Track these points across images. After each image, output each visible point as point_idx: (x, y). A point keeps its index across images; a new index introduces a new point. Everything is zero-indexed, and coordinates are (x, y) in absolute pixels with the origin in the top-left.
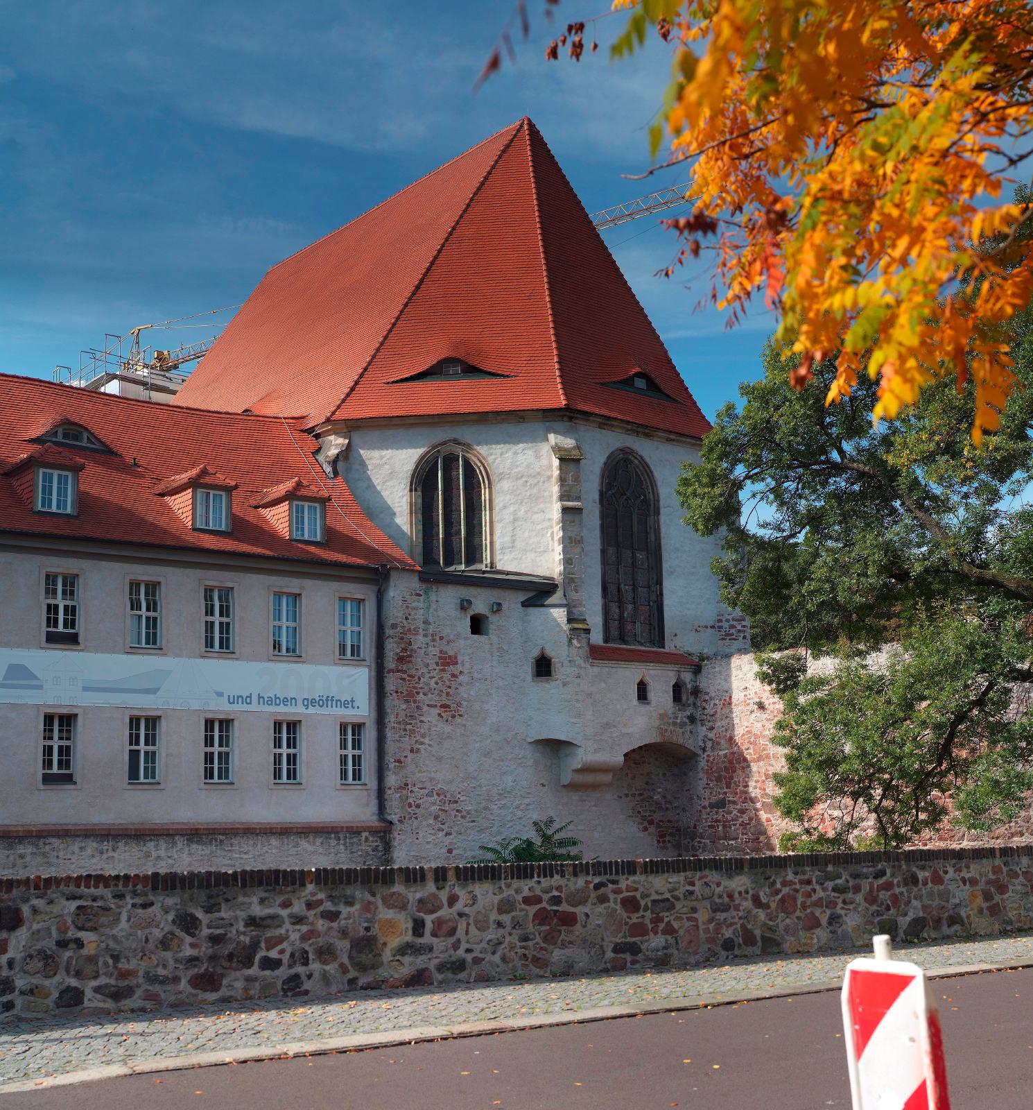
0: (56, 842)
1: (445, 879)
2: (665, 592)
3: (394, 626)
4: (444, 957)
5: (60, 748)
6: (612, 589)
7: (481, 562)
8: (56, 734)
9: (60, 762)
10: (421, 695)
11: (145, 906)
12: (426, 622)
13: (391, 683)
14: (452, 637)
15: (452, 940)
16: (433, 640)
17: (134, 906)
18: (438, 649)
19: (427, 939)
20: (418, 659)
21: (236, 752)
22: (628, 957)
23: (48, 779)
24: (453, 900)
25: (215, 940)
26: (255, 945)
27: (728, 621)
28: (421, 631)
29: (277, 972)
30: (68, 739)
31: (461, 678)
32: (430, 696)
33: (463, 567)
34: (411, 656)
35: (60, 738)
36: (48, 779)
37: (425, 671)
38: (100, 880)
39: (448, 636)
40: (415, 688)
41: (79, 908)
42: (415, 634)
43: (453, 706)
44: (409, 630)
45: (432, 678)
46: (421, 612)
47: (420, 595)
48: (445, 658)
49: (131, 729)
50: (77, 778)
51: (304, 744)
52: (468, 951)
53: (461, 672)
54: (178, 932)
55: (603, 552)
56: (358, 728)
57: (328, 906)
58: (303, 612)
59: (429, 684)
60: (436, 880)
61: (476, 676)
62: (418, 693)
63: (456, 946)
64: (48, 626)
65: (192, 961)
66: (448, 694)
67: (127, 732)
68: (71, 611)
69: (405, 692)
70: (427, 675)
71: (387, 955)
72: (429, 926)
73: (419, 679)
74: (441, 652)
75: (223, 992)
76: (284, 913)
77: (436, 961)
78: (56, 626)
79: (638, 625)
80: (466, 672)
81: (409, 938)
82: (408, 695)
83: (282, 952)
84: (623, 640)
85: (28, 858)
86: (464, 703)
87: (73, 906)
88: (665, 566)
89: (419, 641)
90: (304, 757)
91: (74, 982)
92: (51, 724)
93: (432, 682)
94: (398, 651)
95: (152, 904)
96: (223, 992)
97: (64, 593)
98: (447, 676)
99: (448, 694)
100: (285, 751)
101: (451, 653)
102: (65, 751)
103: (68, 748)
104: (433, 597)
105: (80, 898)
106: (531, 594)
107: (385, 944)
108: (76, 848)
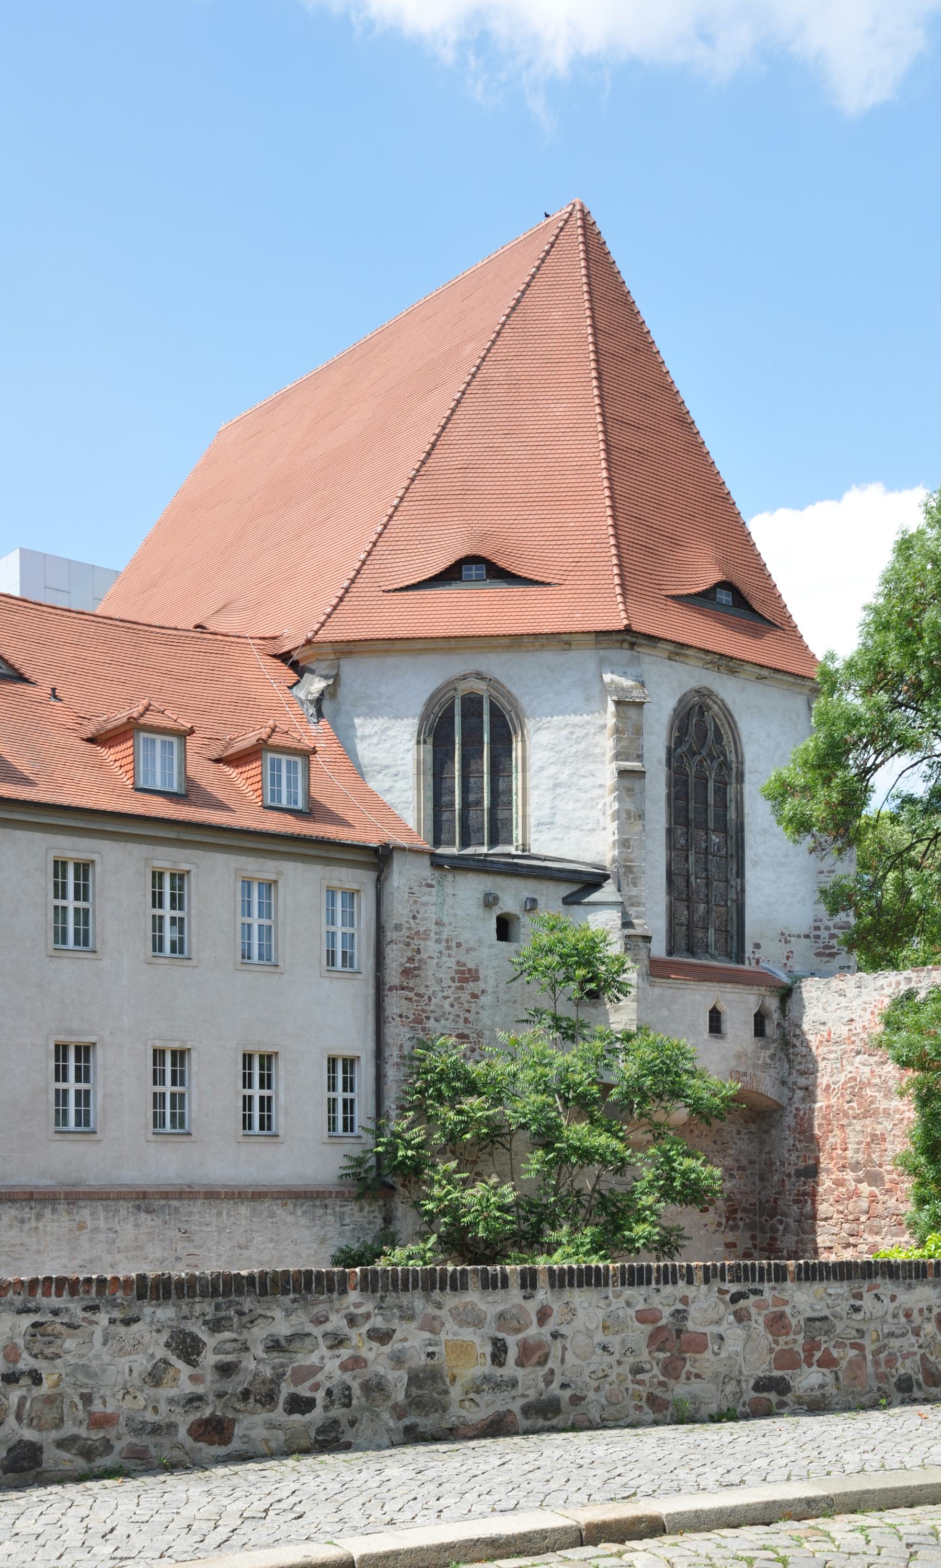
1: (534, 1286)
2: (748, 888)
3: (398, 927)
4: (532, 1394)
6: (680, 882)
7: (510, 842)
10: (432, 1020)
11: (127, 1322)
12: (439, 923)
13: (395, 1004)
14: (472, 944)
15: (543, 1371)
16: (449, 948)
17: (112, 1321)
18: (454, 960)
19: (510, 1369)
20: (430, 972)
21: (195, 1092)
22: (773, 1397)
24: (543, 1315)
25: (226, 1370)
26: (279, 1377)
27: (827, 928)
28: (432, 935)
29: (308, 1417)
31: (484, 1000)
32: (443, 1022)
33: (484, 850)
34: (418, 968)
37: (438, 988)
38: (62, 1285)
39: (466, 942)
40: (424, 1011)
41: (35, 1325)
42: (425, 939)
43: (473, 1036)
44: (418, 933)
45: (446, 998)
46: (433, 908)
47: (431, 886)
48: (462, 972)
49: (57, 1060)
51: (282, 1084)
52: (564, 1386)
53: (483, 992)
54: (173, 1359)
55: (669, 832)
56: (350, 1063)
57: (378, 1322)
58: (280, 905)
59: (442, 1007)
60: (523, 1286)
61: (502, 996)
62: (428, 1018)
63: (548, 1382)
65: (194, 1400)
67: (52, 1064)
69: (412, 1017)
70: (440, 995)
71: (456, 1393)
72: (513, 1353)
73: (430, 999)
74: (458, 963)
75: (236, 1445)
76: (317, 1331)
77: (521, 1402)
79: (711, 931)
80: (490, 990)
81: (487, 1368)
82: (415, 1021)
83: (316, 1387)
84: (691, 952)
86: (487, 1033)
87: (26, 1321)
88: (749, 854)
89: (431, 948)
90: (282, 1100)
91: (29, 1435)
93: (446, 1004)
94: (404, 960)
95: (137, 1320)
96: (236, 1445)
98: (465, 996)
100: (256, 1092)
101: (471, 965)
104: (449, 890)
105: (37, 1310)
106: (575, 888)
107: (454, 1379)
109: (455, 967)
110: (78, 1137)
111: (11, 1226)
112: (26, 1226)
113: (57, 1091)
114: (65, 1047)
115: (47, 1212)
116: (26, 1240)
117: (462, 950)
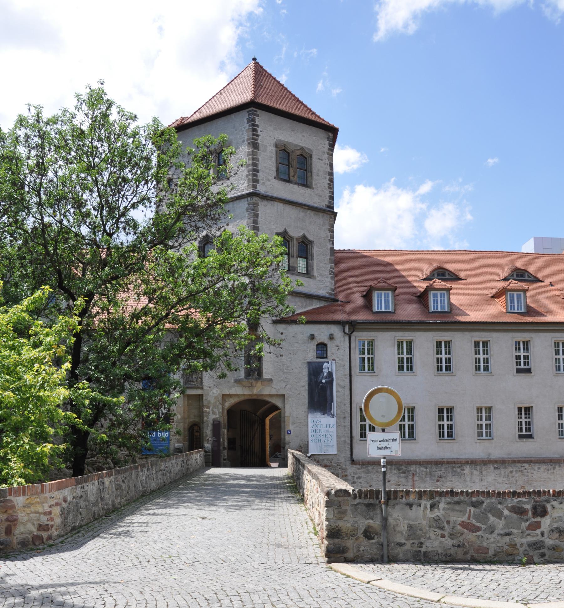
0: (526, 465)
5: (526, 422)
8: (523, 416)
9: (526, 429)
23: (521, 437)
30: (529, 418)
35: (526, 418)
36: (521, 437)
50: (535, 436)
64: (517, 365)
67: (557, 414)
68: (527, 358)
78: (520, 365)
85: (514, 473)
92: (521, 411)
97: (524, 349)
102: (528, 424)
103: (529, 422)
108: (536, 468)
110: (487, 441)
111: (544, 472)
112: (550, 472)
113: (559, 424)
114: (481, 409)
115: (557, 467)
116: (550, 476)
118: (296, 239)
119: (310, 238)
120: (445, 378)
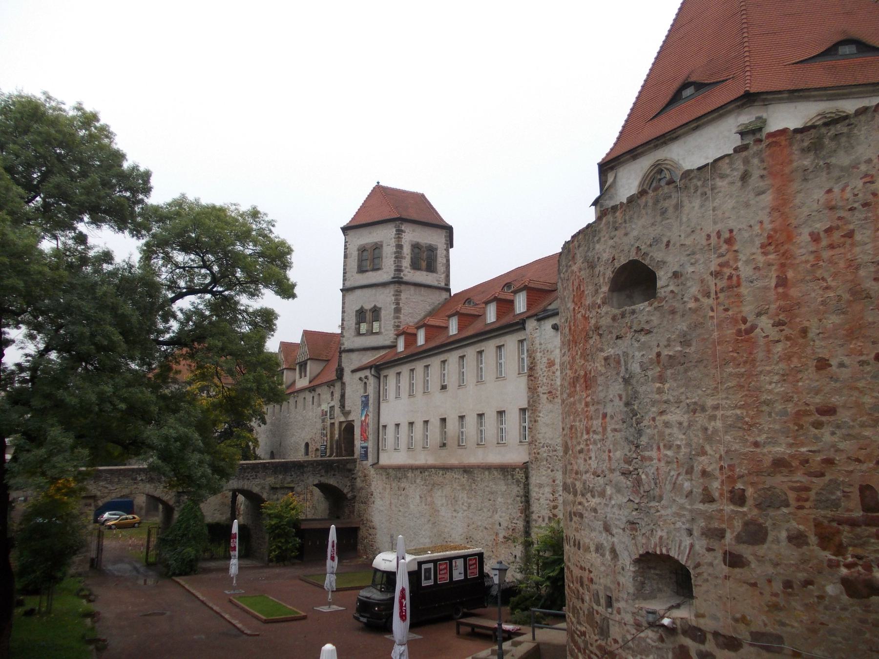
12: (541, 344)
14: (553, 349)
16: (544, 354)
28: (539, 350)
32: (543, 387)
34: (534, 366)
43: (554, 391)
66: (551, 385)
74: (548, 360)
89: (539, 355)
98: (550, 373)
99: (551, 385)
104: (543, 328)
109: (546, 361)
117: (549, 353)
118: (370, 310)
119: (379, 305)
120: (412, 399)
